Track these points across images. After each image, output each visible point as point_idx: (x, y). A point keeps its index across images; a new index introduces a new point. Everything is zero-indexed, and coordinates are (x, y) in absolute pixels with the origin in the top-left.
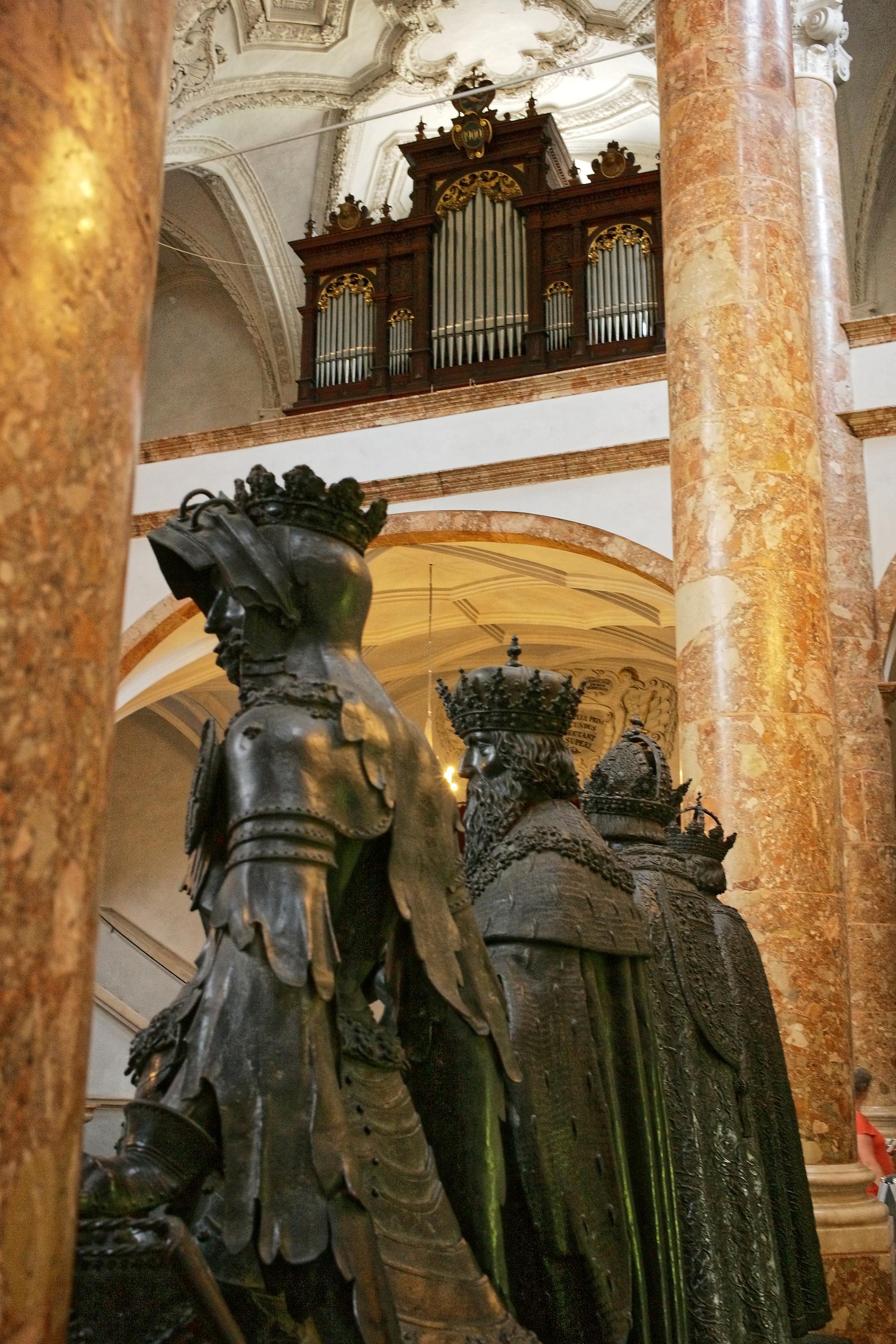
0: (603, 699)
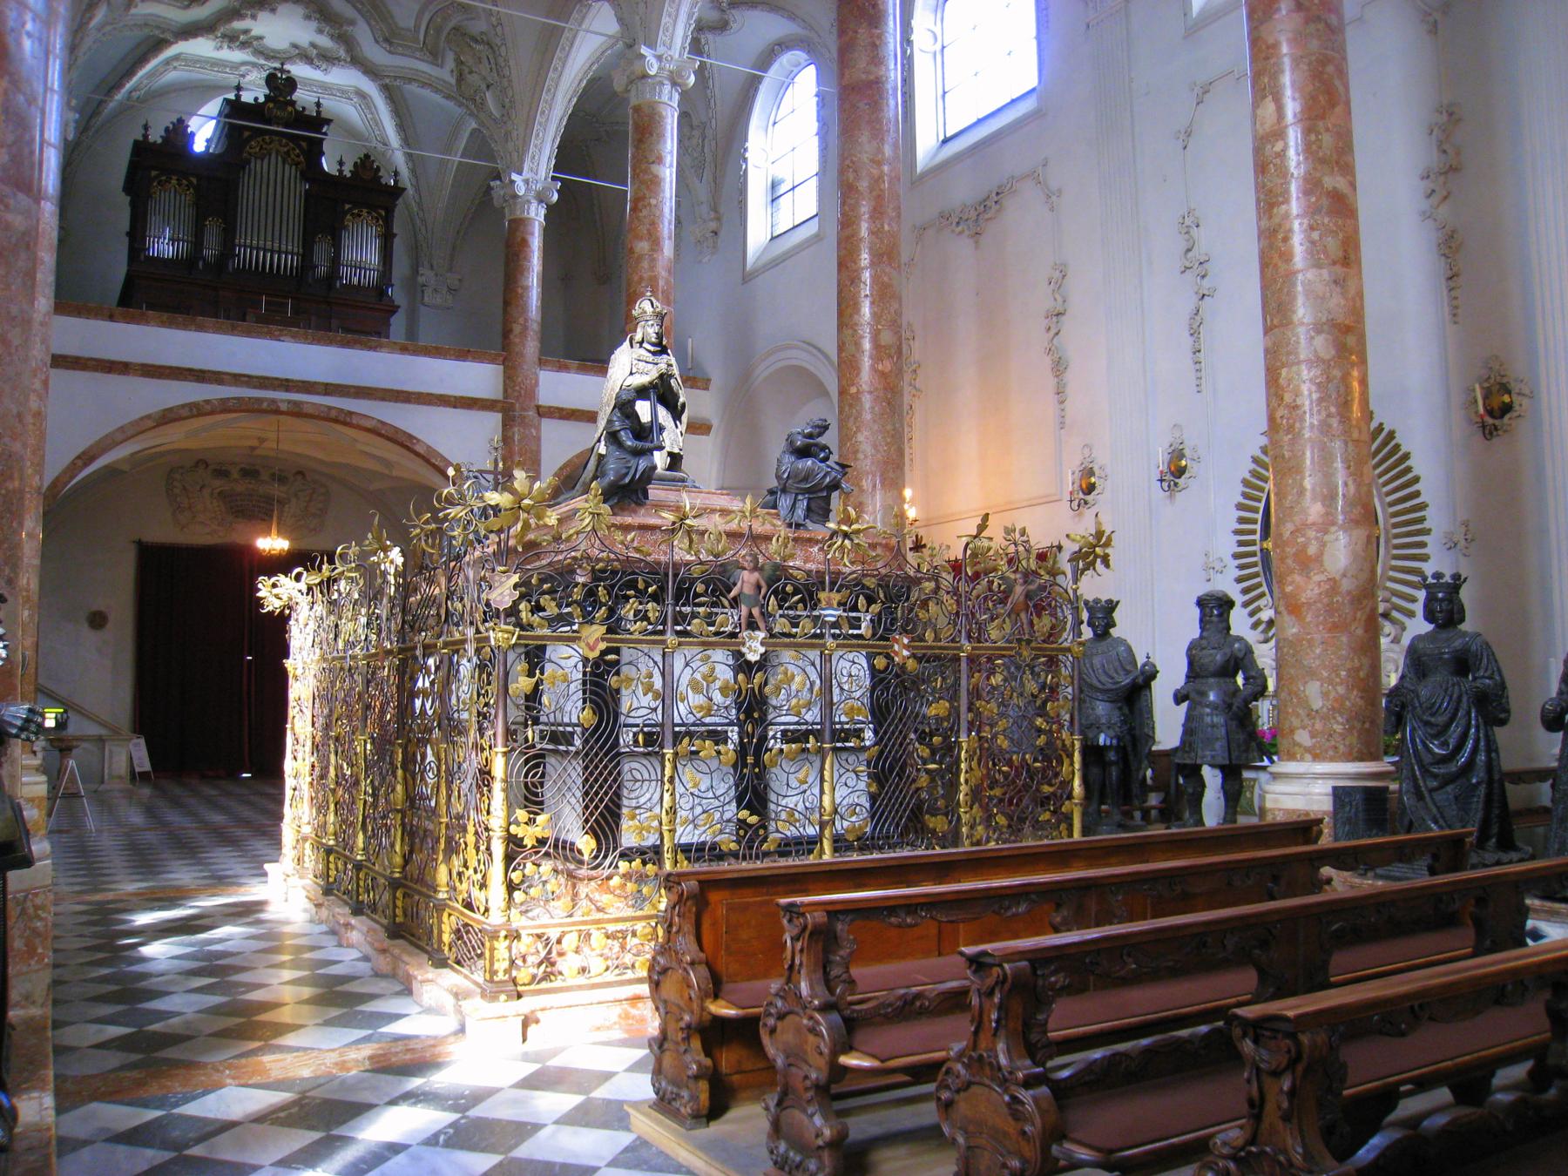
0: (284, 488)
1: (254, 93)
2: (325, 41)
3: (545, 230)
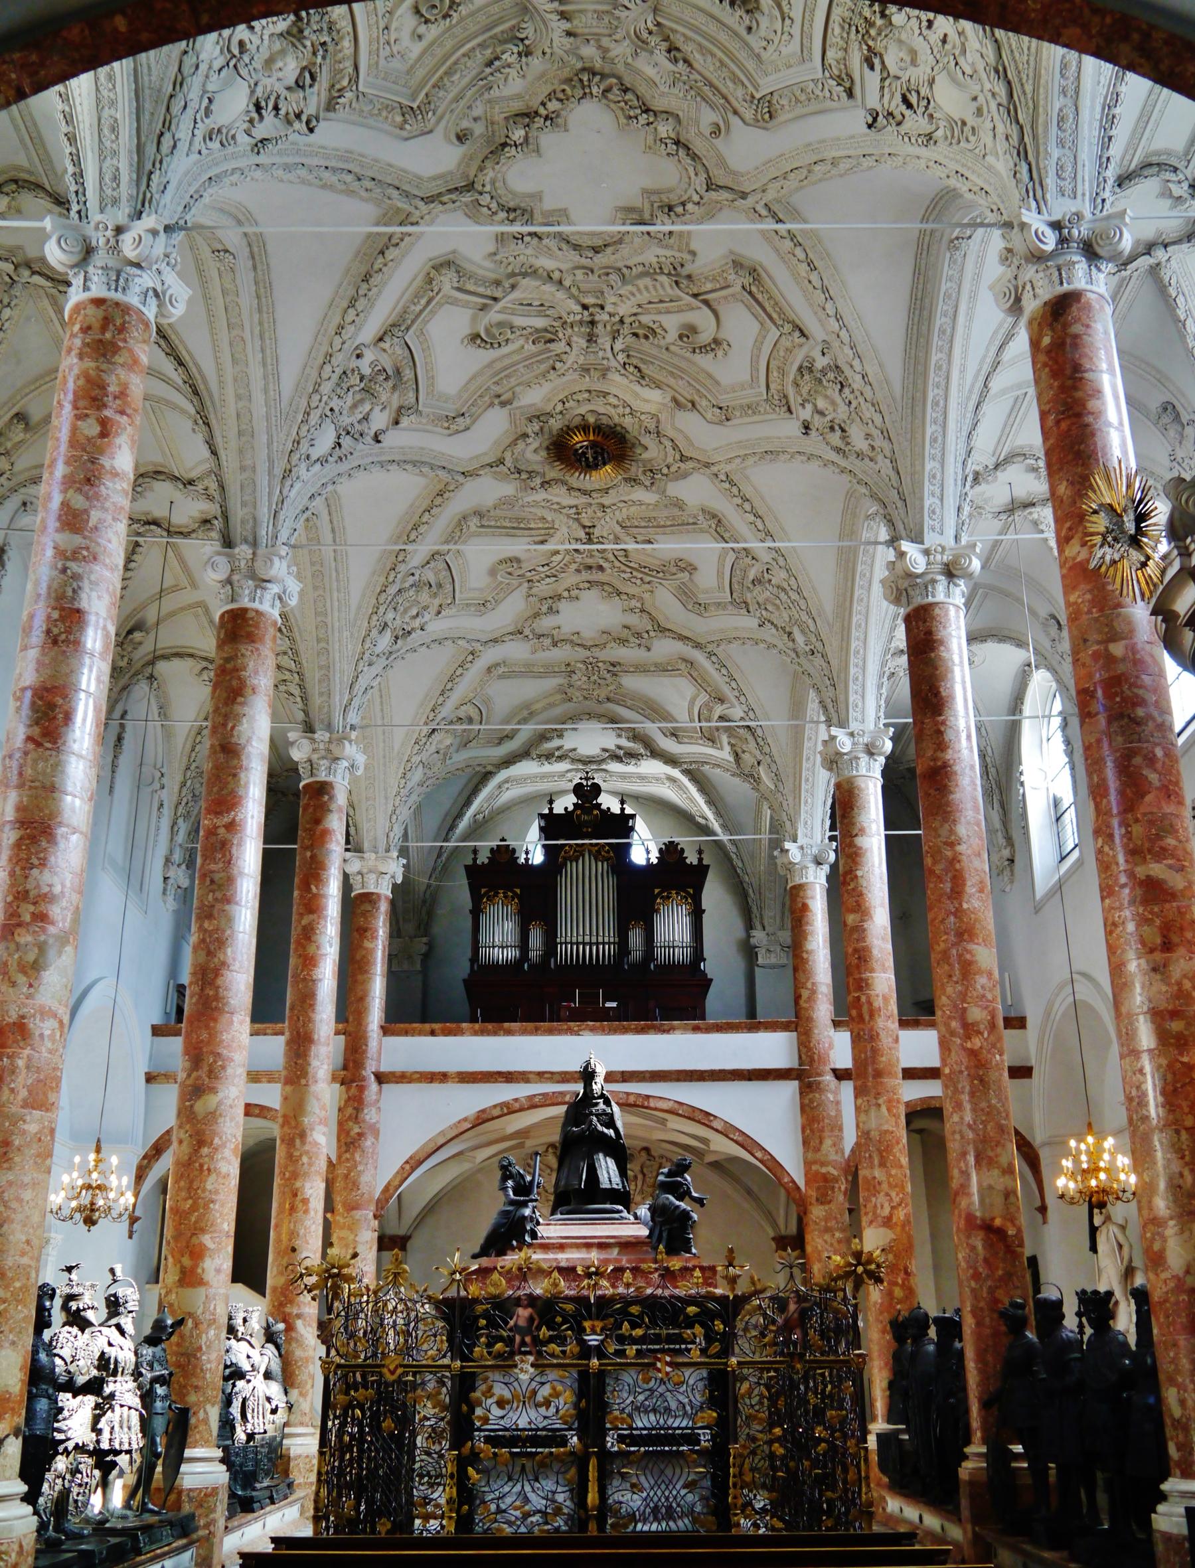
1: (566, 803)
2: (624, 742)
3: (828, 891)
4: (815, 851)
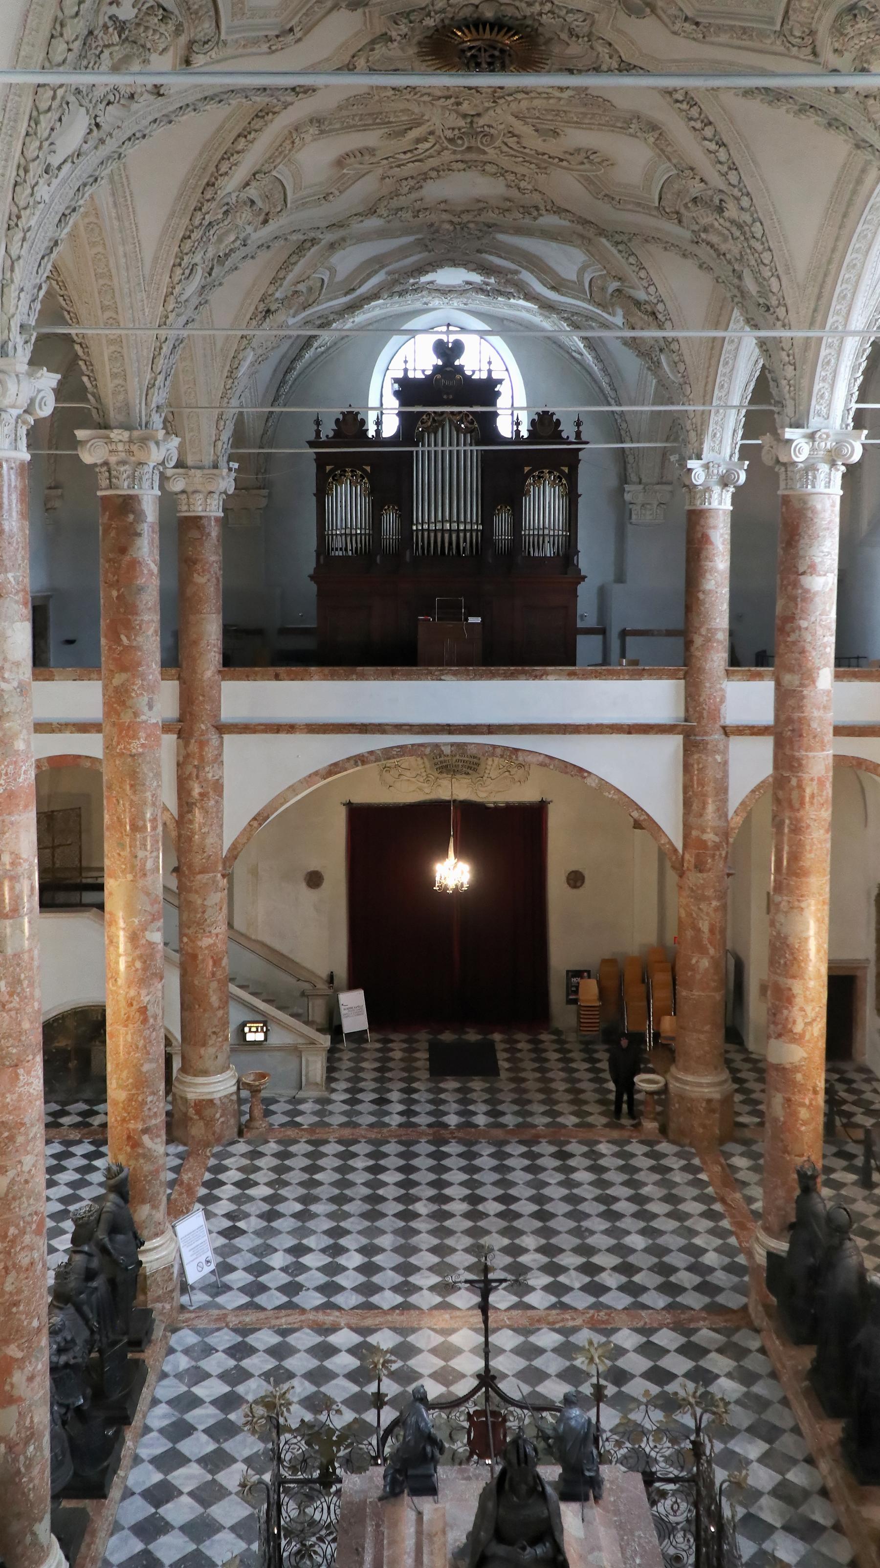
4: (722, 470)
